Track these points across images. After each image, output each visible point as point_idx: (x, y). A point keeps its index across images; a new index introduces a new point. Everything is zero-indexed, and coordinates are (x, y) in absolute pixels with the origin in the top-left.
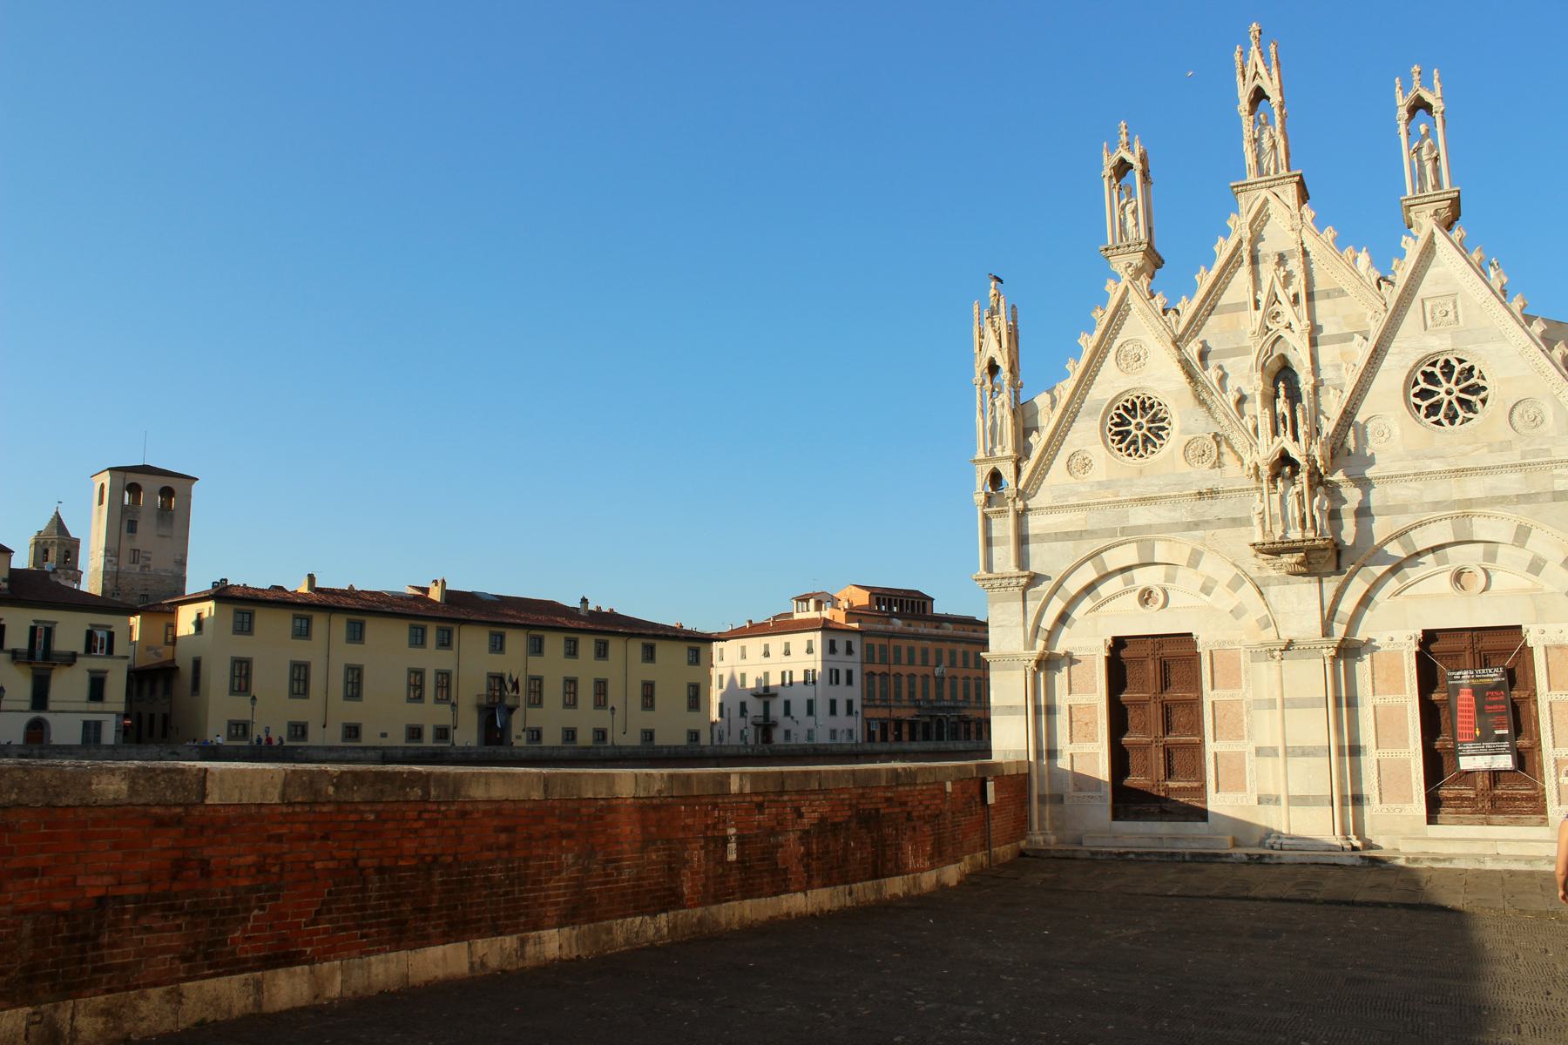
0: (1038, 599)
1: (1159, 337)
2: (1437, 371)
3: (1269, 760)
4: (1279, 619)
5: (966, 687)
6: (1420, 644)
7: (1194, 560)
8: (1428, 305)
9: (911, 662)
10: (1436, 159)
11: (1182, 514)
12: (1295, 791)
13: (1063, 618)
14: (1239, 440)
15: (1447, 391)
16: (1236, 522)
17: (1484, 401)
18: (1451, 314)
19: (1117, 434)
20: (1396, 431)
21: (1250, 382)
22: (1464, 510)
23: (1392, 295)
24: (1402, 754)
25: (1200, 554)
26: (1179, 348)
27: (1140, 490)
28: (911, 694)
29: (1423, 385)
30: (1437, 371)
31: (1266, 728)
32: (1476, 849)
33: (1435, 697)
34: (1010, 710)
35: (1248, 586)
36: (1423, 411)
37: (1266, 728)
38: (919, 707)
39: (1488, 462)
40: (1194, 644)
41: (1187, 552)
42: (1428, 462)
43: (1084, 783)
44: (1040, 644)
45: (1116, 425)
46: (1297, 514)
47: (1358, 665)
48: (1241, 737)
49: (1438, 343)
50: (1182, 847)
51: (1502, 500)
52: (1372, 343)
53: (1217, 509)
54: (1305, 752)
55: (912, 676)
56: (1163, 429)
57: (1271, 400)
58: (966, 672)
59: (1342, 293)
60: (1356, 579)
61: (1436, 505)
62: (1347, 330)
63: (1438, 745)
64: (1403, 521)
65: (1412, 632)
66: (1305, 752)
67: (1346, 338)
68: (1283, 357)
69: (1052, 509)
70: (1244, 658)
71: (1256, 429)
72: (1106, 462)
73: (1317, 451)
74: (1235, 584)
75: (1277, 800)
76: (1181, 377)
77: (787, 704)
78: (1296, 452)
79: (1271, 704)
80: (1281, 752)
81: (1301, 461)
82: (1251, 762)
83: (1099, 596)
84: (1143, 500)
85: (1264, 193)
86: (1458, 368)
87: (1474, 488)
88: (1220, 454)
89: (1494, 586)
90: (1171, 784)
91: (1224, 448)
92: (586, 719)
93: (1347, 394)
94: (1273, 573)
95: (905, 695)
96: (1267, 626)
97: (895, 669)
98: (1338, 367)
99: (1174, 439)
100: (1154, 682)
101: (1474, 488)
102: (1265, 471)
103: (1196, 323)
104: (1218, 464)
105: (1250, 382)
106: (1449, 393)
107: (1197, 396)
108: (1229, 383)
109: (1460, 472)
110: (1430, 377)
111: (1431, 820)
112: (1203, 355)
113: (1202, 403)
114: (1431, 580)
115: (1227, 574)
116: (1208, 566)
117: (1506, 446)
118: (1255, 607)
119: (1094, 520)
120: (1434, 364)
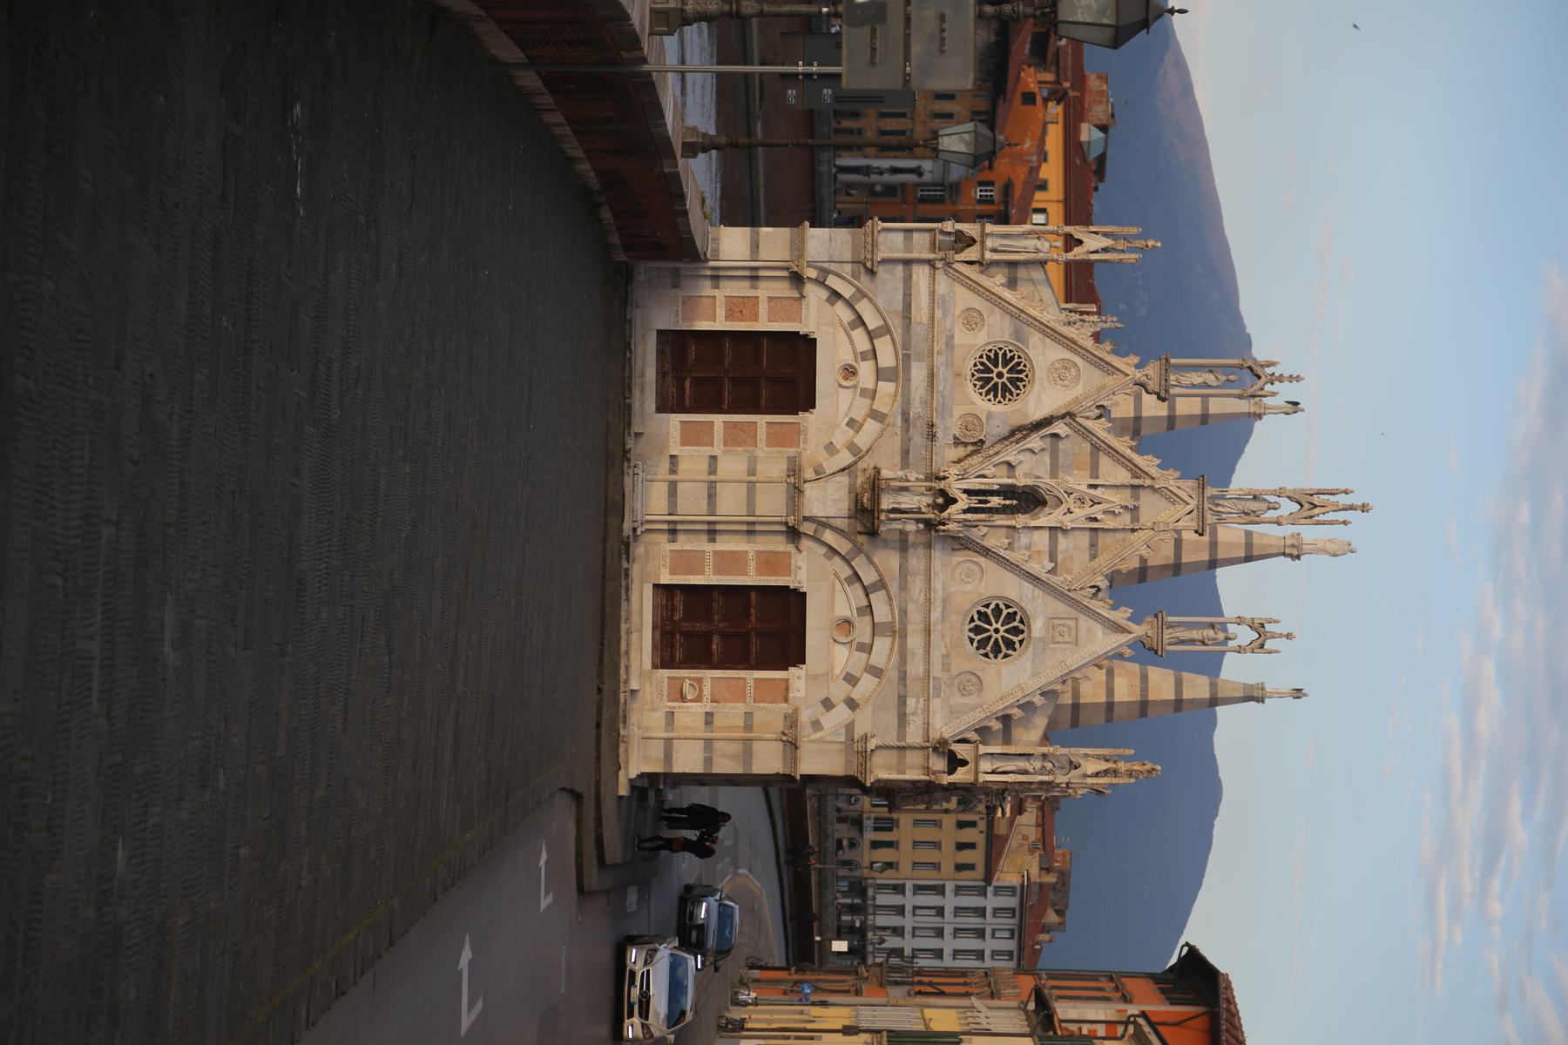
0: (853, 276)
1: (1076, 400)
2: (1015, 624)
3: (705, 467)
4: (821, 483)
6: (795, 590)
7: (875, 415)
8: (1072, 623)
10: (1203, 643)
11: (916, 408)
12: (680, 486)
13: (835, 295)
14: (977, 459)
15: (998, 631)
16: (905, 453)
17: (986, 655)
18: (1060, 639)
19: (996, 354)
20: (969, 588)
21: (1026, 475)
22: (898, 632)
23: (1084, 597)
24: (709, 570)
25: (881, 422)
26: (1063, 417)
27: (941, 372)
29: (1005, 612)
30: (1015, 624)
31: (732, 466)
32: (635, 618)
33: (753, 595)
34: (755, 246)
35: (851, 459)
36: (983, 610)
37: (732, 466)
39: (936, 656)
40: (805, 410)
41: (885, 410)
42: (939, 610)
43: (690, 303)
44: (812, 273)
45: (1005, 354)
46: (903, 506)
47: (782, 538)
48: (725, 444)
49: (1038, 627)
50: (636, 392)
52: (1044, 576)
53: (918, 439)
54: (712, 496)
56: (995, 396)
57: (1007, 491)
59: (1093, 557)
60: (850, 546)
61: (904, 612)
62: (1060, 557)
63: (715, 595)
64: (894, 587)
65: (805, 584)
66: (712, 496)
67: (1053, 557)
68: (1043, 503)
69: (932, 293)
70: (791, 451)
71: (984, 476)
72: (972, 343)
73: (951, 526)
74: (852, 448)
75: (673, 472)
76: (1037, 414)
78: (953, 509)
79: (752, 472)
80: (713, 478)
81: (945, 514)
82: (705, 451)
83: (853, 329)
84: (932, 376)
85: (1193, 504)
86: (1015, 639)
87: (915, 641)
88: (965, 444)
89: (837, 647)
90: (688, 383)
91: (970, 448)
93: (1002, 553)
94: (859, 481)
96: (817, 473)
98: (1028, 547)
99: (983, 405)
100: (774, 374)
102: (942, 485)
103: (1086, 434)
104: (957, 442)
105: (1026, 475)
106: (997, 631)
107: (1020, 429)
108: (1028, 454)
109: (928, 632)
110: (1011, 617)
111: (657, 587)
112: (1056, 436)
113: (1012, 433)
114: (846, 603)
115: (863, 441)
116: (871, 427)
117: (946, 667)
118: (832, 464)
119: (918, 331)
120: (1021, 621)
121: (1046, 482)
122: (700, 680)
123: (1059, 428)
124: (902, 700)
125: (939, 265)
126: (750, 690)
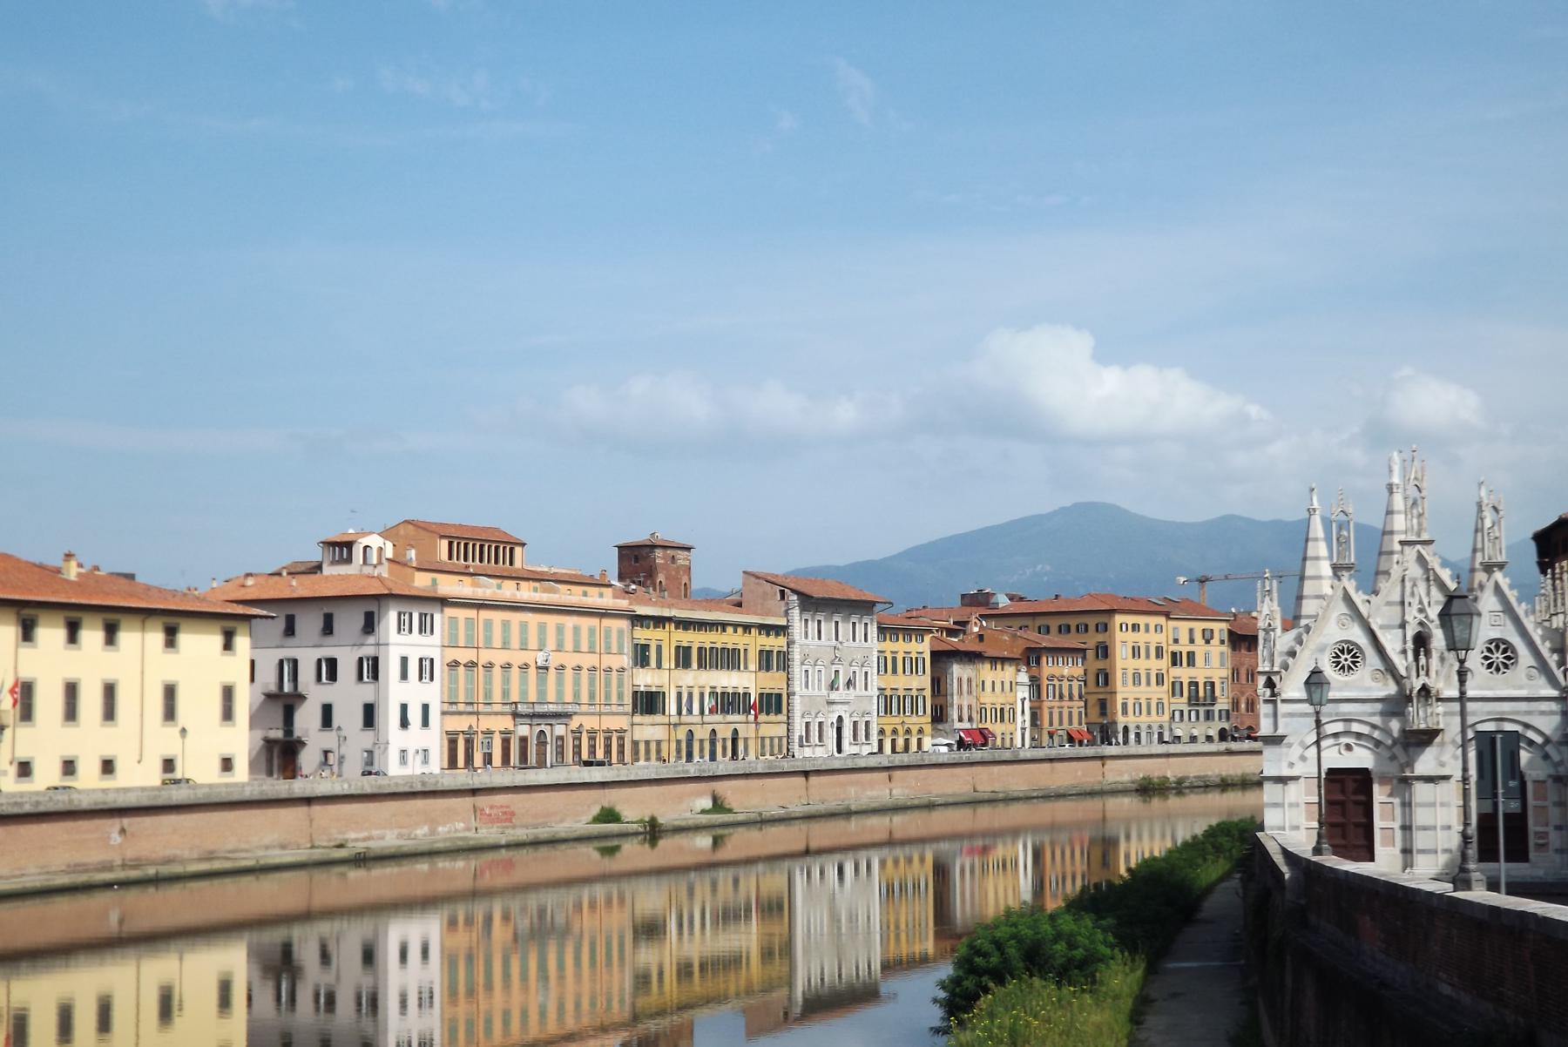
2: (1492, 646)
5: (577, 683)
9: (505, 646)
21: (1405, 642)
28: (506, 693)
30: (1492, 646)
38: (515, 715)
51: (1517, 713)
54: (1425, 828)
55: (507, 667)
58: (576, 659)
61: (1489, 713)
66: (1425, 828)
77: (327, 710)
92: (89, 739)
95: (497, 696)
97: (485, 657)
101: (1506, 706)
117: (1521, 687)
121: (1410, 634)
122: (1536, 833)
123: (1374, 627)
124: (1542, 713)
125: (1284, 696)
126: (1539, 803)
